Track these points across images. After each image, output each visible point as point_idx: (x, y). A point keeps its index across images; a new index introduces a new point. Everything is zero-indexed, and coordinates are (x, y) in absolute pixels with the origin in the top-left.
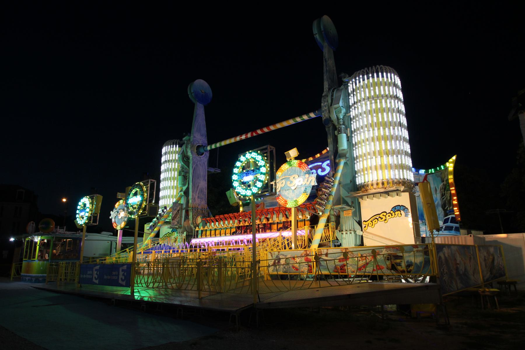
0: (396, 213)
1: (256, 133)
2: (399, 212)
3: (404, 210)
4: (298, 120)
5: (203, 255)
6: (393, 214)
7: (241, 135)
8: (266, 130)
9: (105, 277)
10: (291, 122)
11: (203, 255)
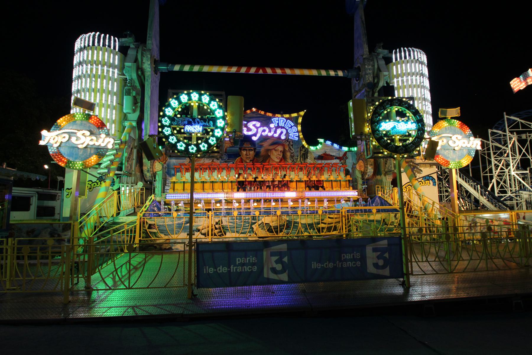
0: (426, 182)
1: (265, 71)
2: (428, 181)
3: (432, 180)
4: (324, 73)
5: (329, 218)
6: (424, 183)
7: (240, 66)
8: (279, 71)
9: (314, 265)
10: (314, 73)
11: (329, 218)
